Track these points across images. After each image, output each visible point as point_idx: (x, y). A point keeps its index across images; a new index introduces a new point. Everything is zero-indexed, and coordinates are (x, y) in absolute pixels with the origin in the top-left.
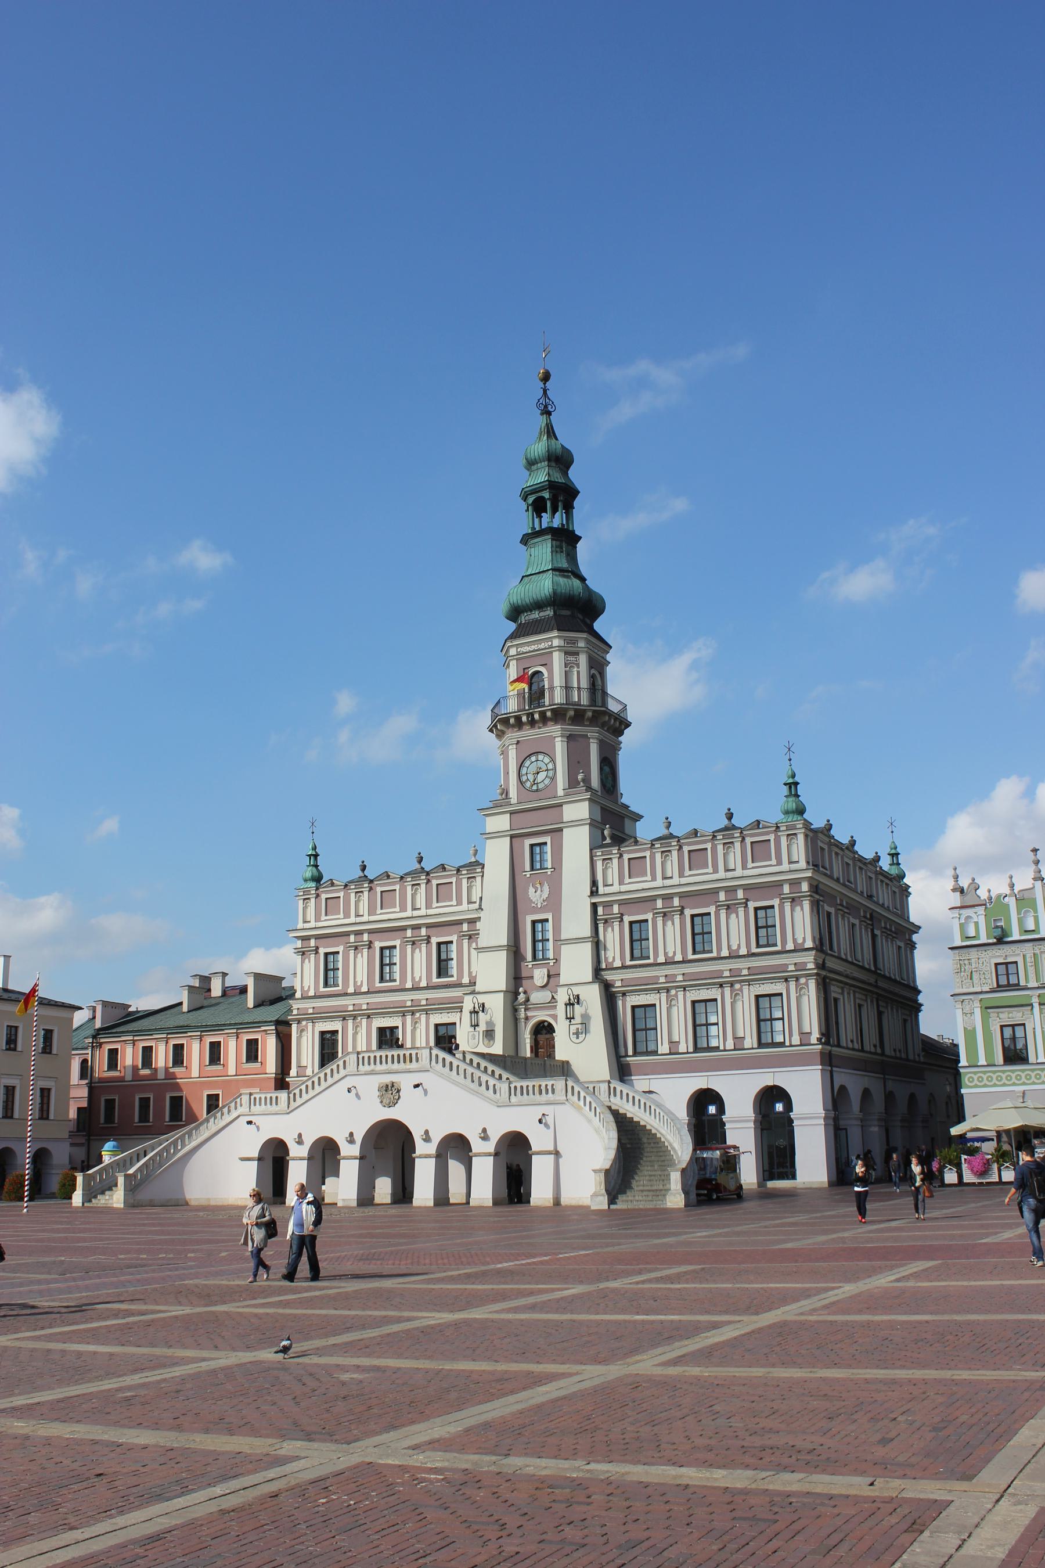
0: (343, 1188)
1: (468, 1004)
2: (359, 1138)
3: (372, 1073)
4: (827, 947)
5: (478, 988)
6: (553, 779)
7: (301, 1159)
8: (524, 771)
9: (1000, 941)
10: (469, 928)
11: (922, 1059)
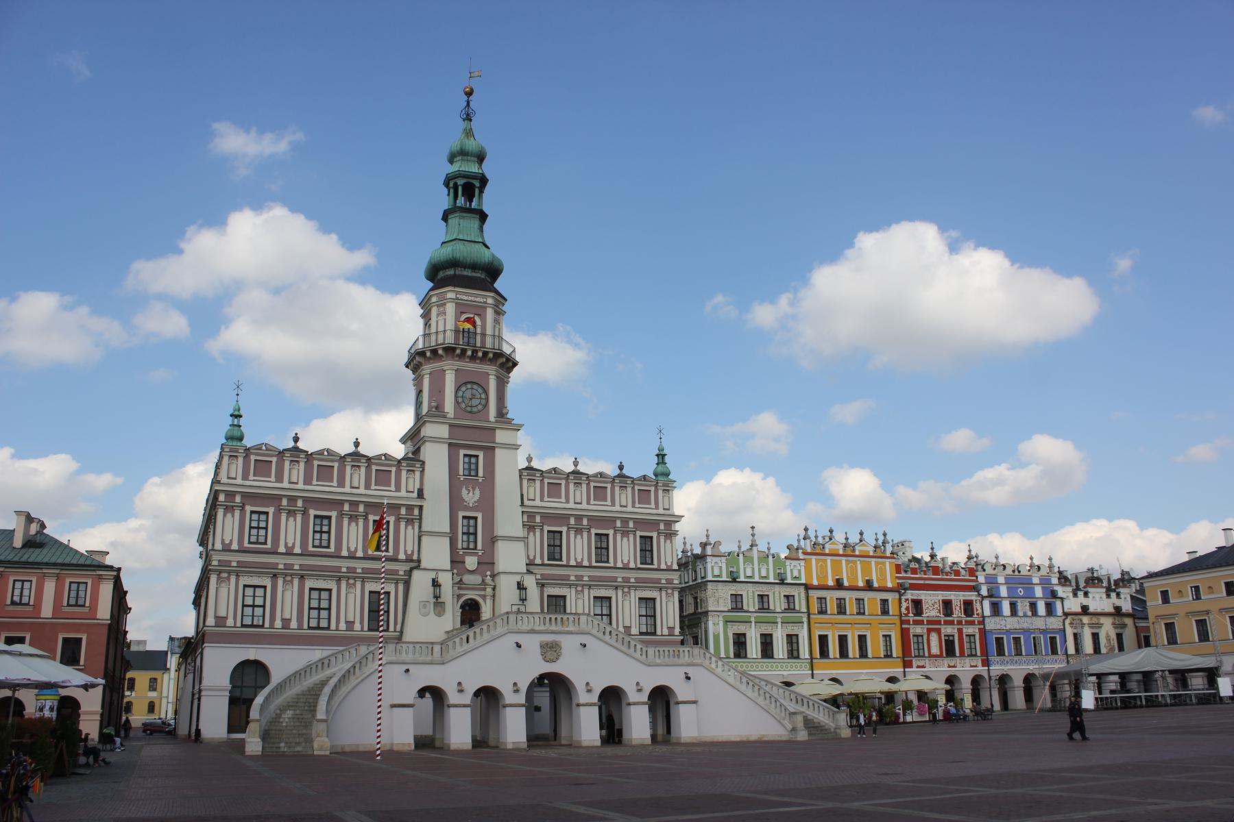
0: (514, 728)
2: (524, 687)
3: (533, 631)
5: (423, 565)
6: (486, 405)
7: (465, 706)
8: (460, 394)
9: (734, 581)
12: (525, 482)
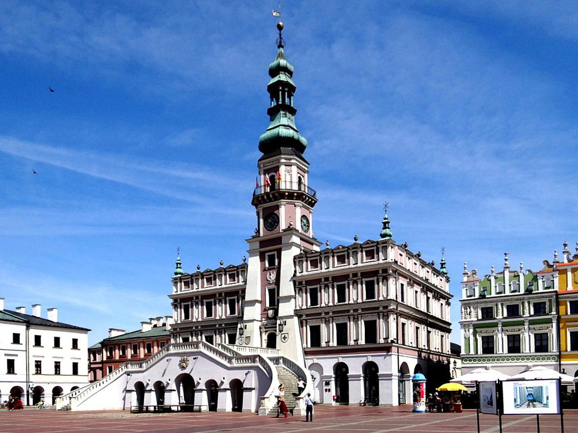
1: (239, 326)
4: (399, 300)
5: (245, 318)
10: (240, 293)
11: (450, 353)
12: (297, 263)
